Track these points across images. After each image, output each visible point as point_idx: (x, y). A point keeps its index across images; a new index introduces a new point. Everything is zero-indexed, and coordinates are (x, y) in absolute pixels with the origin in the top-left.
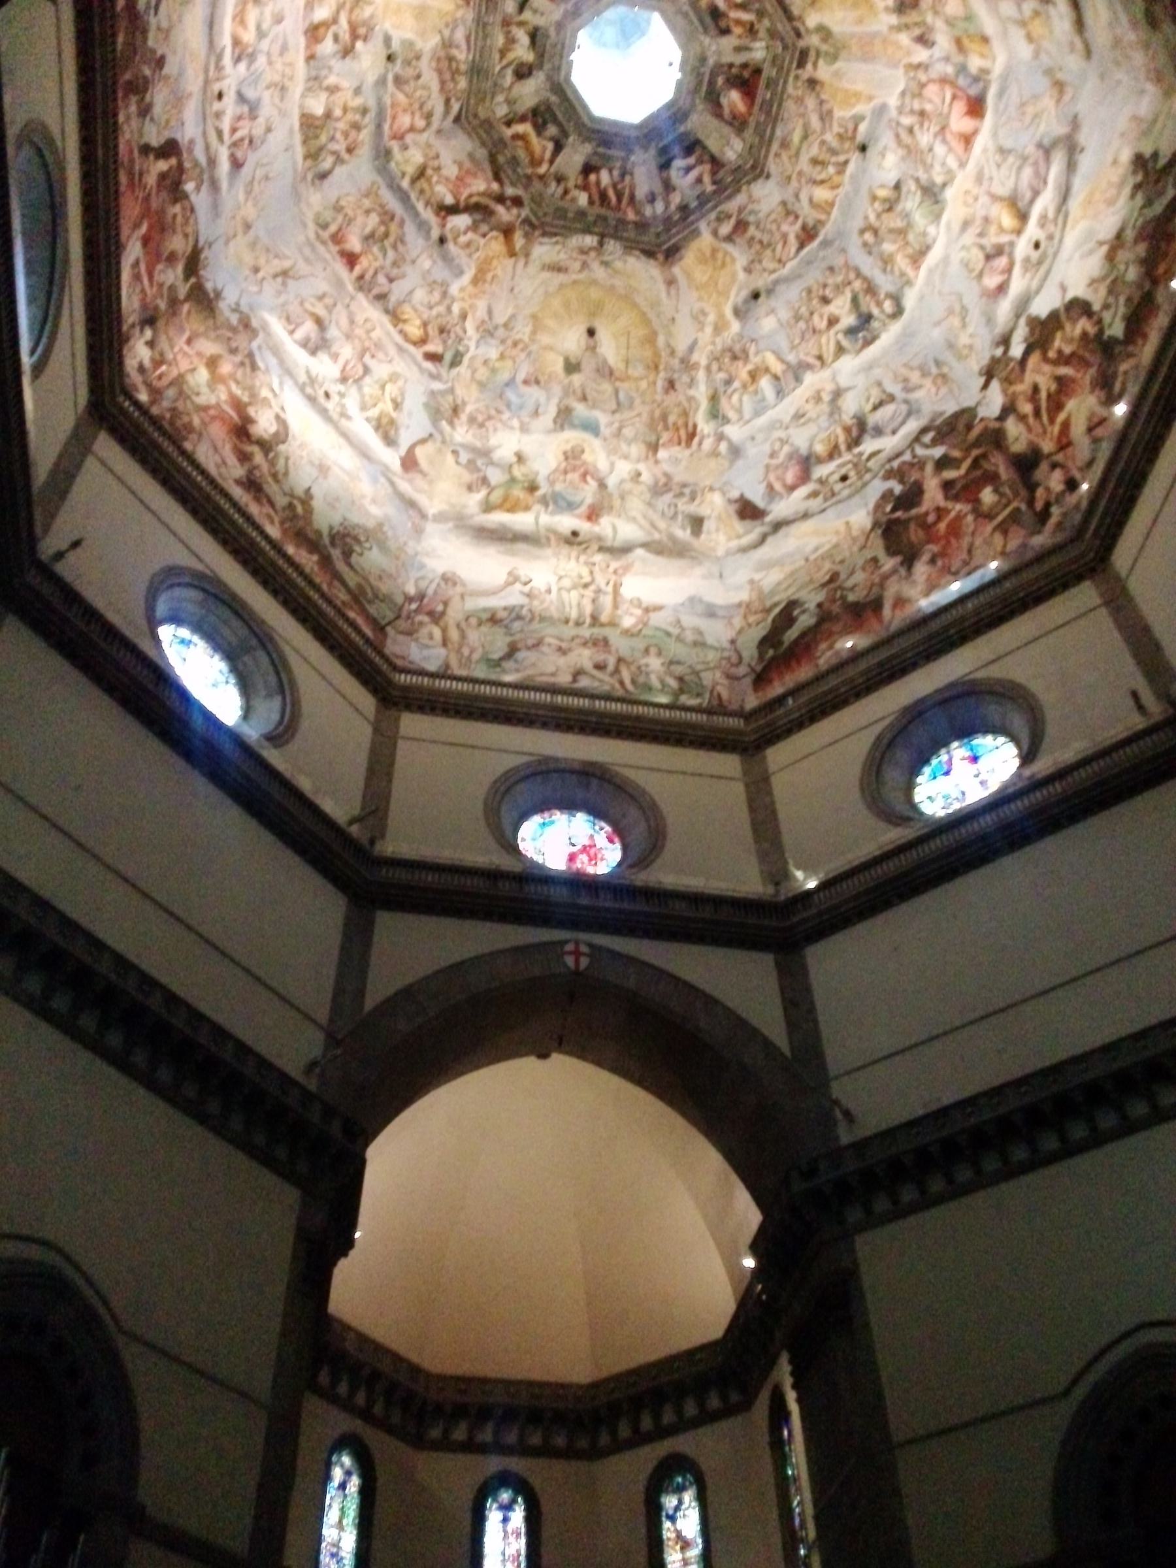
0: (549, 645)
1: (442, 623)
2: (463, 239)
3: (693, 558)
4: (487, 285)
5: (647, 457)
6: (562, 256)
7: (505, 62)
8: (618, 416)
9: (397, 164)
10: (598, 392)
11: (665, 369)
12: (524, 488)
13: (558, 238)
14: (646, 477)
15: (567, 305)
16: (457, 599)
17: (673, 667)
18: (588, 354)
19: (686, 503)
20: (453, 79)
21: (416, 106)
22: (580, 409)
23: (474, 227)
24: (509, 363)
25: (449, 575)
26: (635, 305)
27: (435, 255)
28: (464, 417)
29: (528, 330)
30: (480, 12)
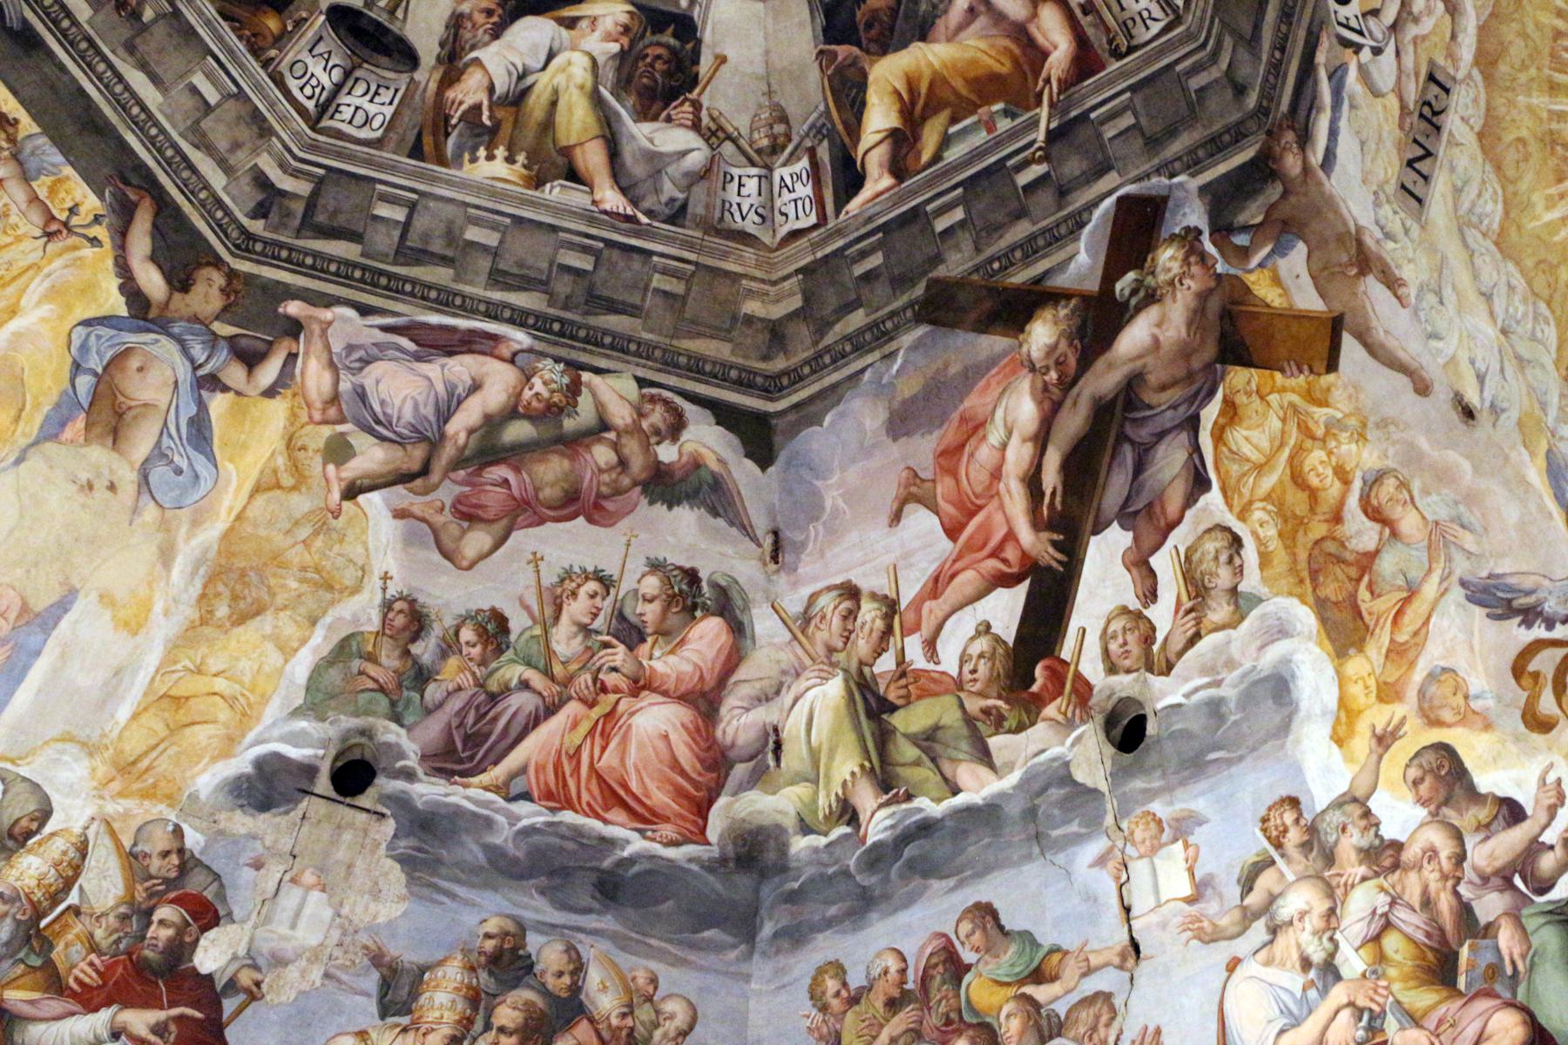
2: (1162, 615)
4: (1387, 564)
6: (1385, 70)
7: (593, 158)
9: (806, 829)
13: (1321, 57)
20: (574, 443)
21: (619, 654)
27: (1158, 807)
30: (344, 272)
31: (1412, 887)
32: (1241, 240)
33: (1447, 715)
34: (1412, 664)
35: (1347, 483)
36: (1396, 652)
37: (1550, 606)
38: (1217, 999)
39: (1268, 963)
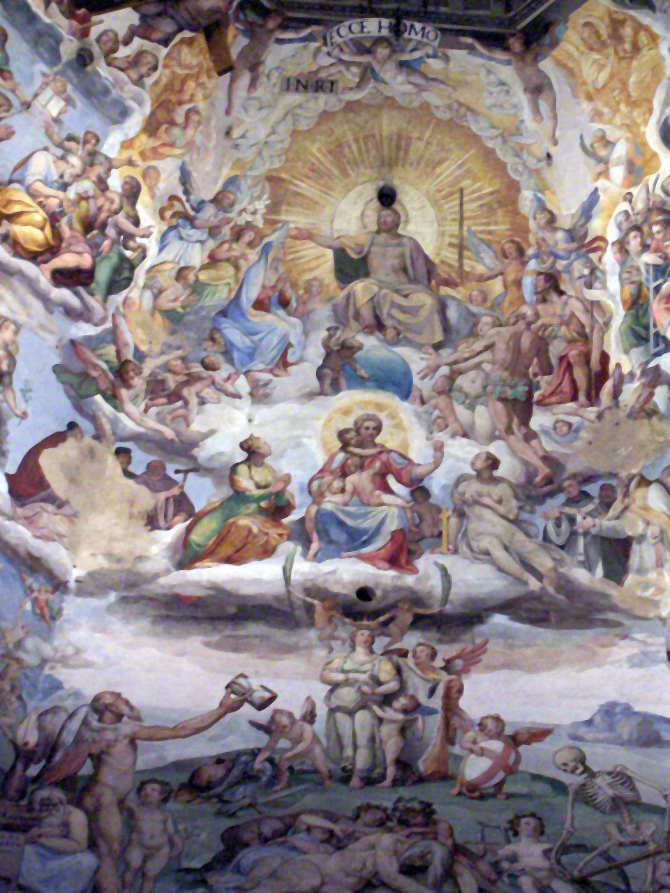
0: (309, 829)
1: (89, 802)
2: (123, 52)
3: (607, 623)
4: (176, 131)
5: (509, 430)
8: (446, 354)
10: (403, 309)
11: (536, 256)
12: (261, 511)
13: (314, 28)
14: (508, 468)
15: (337, 151)
16: (122, 747)
17: (564, 859)
18: (384, 235)
19: (590, 514)
22: (371, 346)
23: (143, 30)
24: (227, 271)
25: (108, 700)
26: (475, 136)
27: (69, 88)
28: (139, 383)
29: (261, 205)
31: (101, 201)
32: (241, 16)
33: (148, 181)
34: (154, 159)
35: (191, 100)
36: (154, 150)
37: (192, 197)
38: (34, 150)
39: (54, 162)
